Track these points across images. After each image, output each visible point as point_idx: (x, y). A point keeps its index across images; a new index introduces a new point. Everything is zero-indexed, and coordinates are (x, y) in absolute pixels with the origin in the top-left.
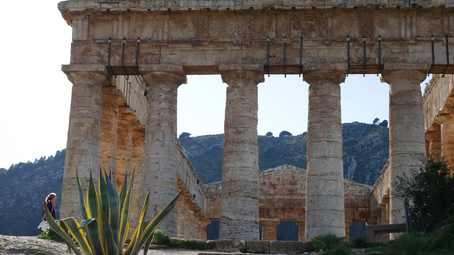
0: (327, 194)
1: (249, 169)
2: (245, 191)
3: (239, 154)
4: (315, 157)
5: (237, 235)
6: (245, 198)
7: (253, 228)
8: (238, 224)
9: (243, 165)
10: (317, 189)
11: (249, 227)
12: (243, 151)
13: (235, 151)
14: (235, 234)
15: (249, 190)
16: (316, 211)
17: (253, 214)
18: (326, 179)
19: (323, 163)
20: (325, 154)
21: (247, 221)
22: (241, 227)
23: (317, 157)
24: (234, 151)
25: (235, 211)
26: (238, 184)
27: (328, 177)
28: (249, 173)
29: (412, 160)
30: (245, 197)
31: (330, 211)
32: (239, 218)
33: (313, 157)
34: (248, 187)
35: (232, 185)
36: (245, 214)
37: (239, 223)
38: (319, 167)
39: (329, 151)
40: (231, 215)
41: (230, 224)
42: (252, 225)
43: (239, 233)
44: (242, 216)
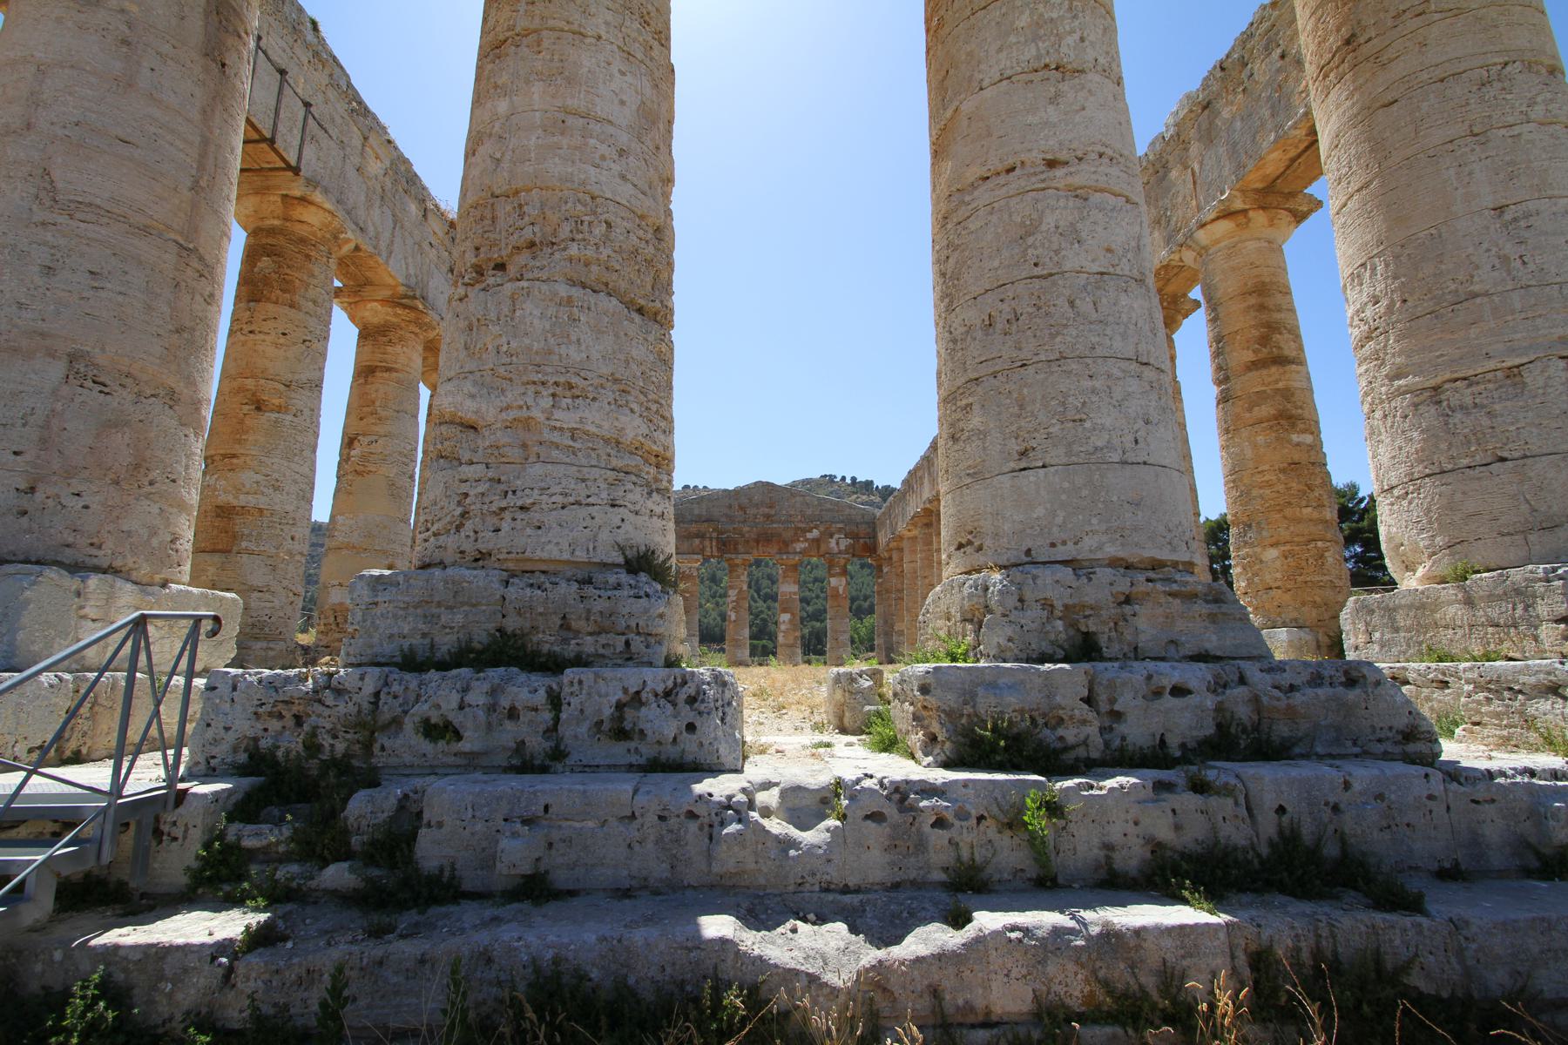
0: (1095, 268)
1: (610, 130)
2: (574, 250)
3: (546, 44)
4: (997, 77)
5: (506, 526)
6: (576, 292)
7: (630, 486)
8: (514, 454)
9: (569, 102)
10: (1030, 240)
11: (595, 473)
12: (575, 27)
13: (527, 33)
14: (492, 521)
15: (605, 252)
16: (1031, 370)
17: (630, 398)
18: (1076, 180)
19: (1053, 100)
20: (1058, 51)
21: (586, 433)
22: (538, 469)
23: (1008, 73)
24: (518, 30)
25: (502, 370)
26: (532, 211)
27: (1093, 169)
28: (603, 149)
29: (1549, 96)
30: (572, 282)
31: (1124, 365)
32: (524, 413)
33: (985, 84)
34: (600, 230)
35: (494, 219)
36: (571, 387)
37: (524, 446)
38: (1030, 119)
39: (1082, 39)
40: (473, 396)
41: (466, 456)
42: (615, 463)
43: (520, 515)
44: (546, 402)
